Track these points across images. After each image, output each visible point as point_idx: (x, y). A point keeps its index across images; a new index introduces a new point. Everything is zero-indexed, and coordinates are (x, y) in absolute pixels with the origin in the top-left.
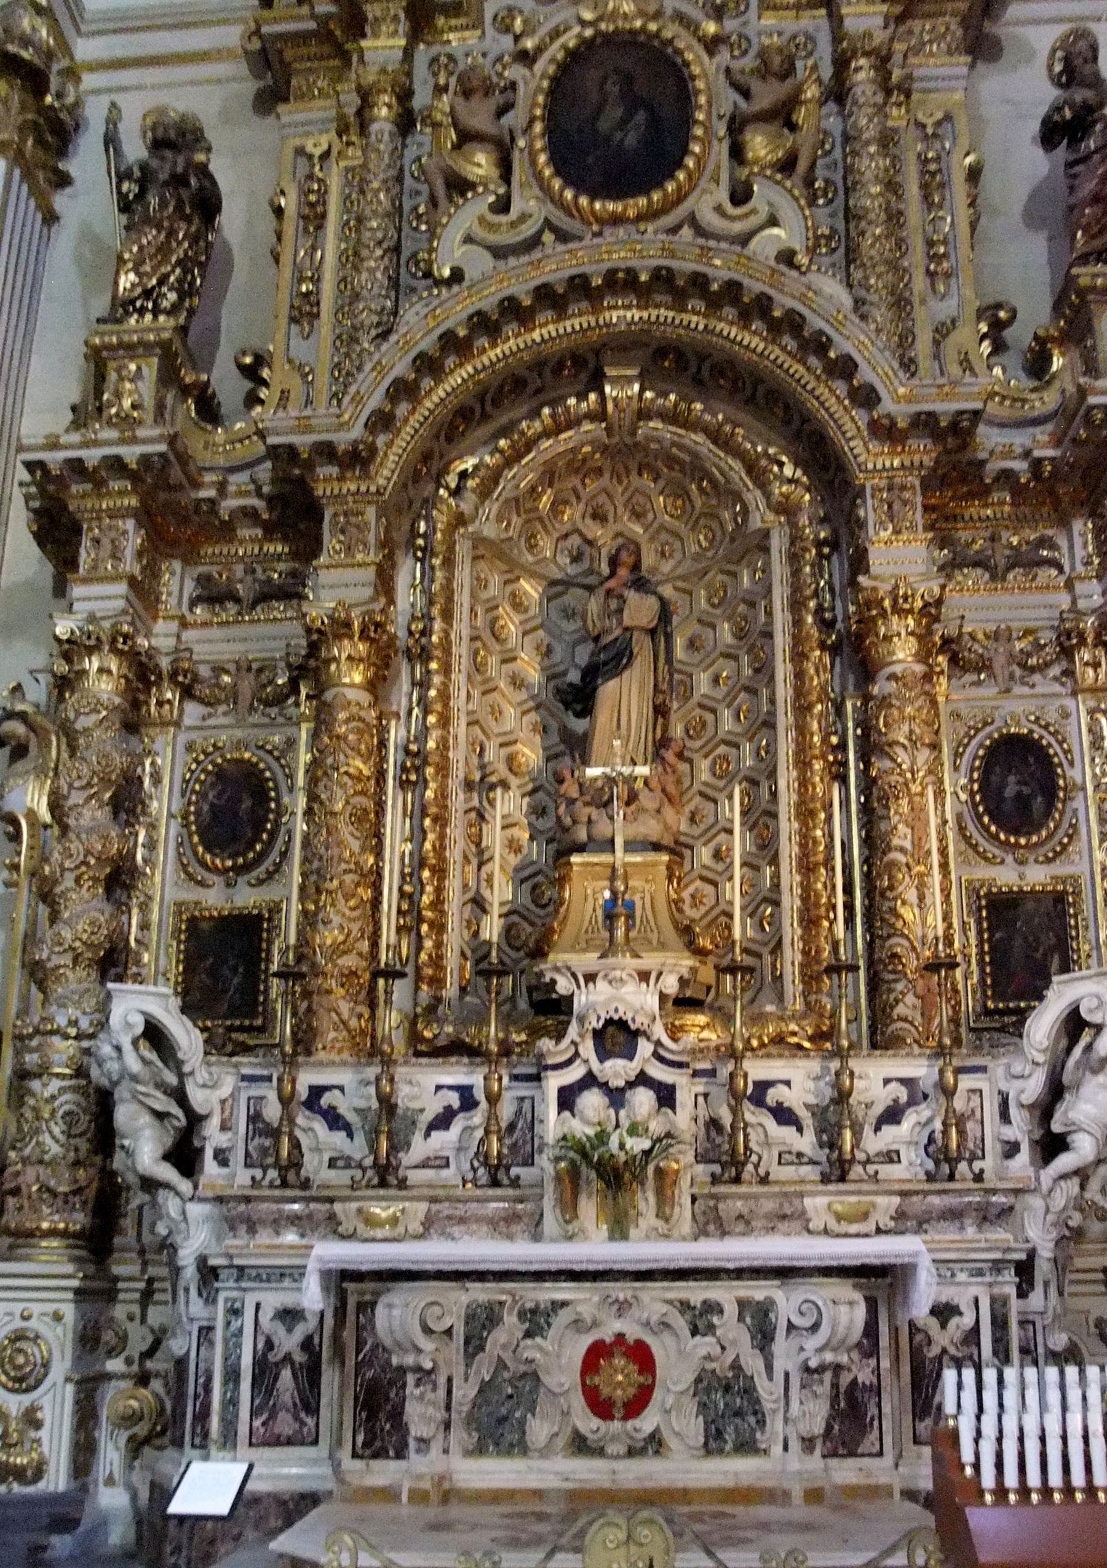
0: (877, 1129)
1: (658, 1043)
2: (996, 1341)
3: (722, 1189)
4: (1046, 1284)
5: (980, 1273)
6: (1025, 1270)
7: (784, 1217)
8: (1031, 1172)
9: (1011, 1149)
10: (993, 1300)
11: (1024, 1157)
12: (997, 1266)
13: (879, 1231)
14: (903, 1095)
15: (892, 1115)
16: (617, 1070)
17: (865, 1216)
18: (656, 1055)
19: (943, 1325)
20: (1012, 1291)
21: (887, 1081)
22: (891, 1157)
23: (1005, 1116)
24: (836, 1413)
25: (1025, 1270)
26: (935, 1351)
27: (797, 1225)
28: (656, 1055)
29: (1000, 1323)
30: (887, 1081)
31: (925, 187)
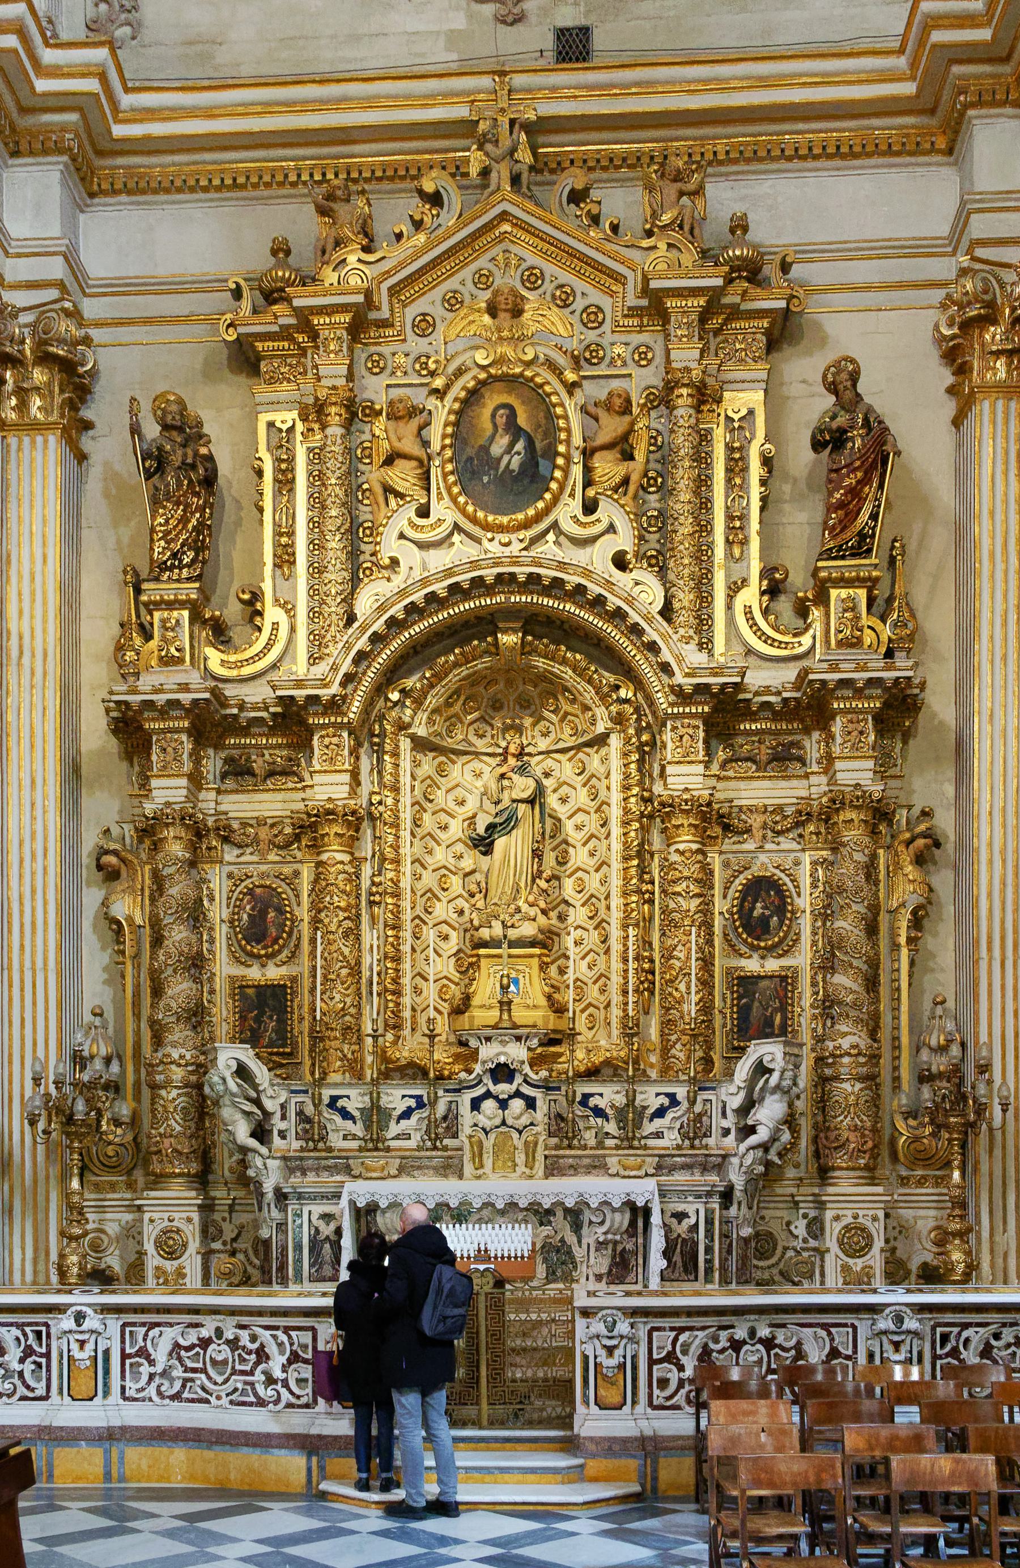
0: (651, 1120)
1: (526, 1075)
2: (707, 1231)
3: (561, 1152)
4: (739, 1203)
5: (700, 1197)
6: (727, 1196)
7: (595, 1167)
8: (734, 1144)
9: (726, 1132)
10: (706, 1210)
11: (732, 1136)
12: (709, 1194)
13: (647, 1175)
14: (666, 1102)
15: (660, 1113)
16: (503, 1089)
17: (640, 1168)
18: (525, 1081)
19: (680, 1223)
20: (717, 1206)
21: (658, 1095)
22: (659, 1135)
23: (724, 1115)
24: (613, 1264)
25: (727, 1196)
26: (675, 1235)
27: (602, 1171)
28: (525, 1081)
29: (710, 1222)
30: (658, 1095)
31: (729, 470)
